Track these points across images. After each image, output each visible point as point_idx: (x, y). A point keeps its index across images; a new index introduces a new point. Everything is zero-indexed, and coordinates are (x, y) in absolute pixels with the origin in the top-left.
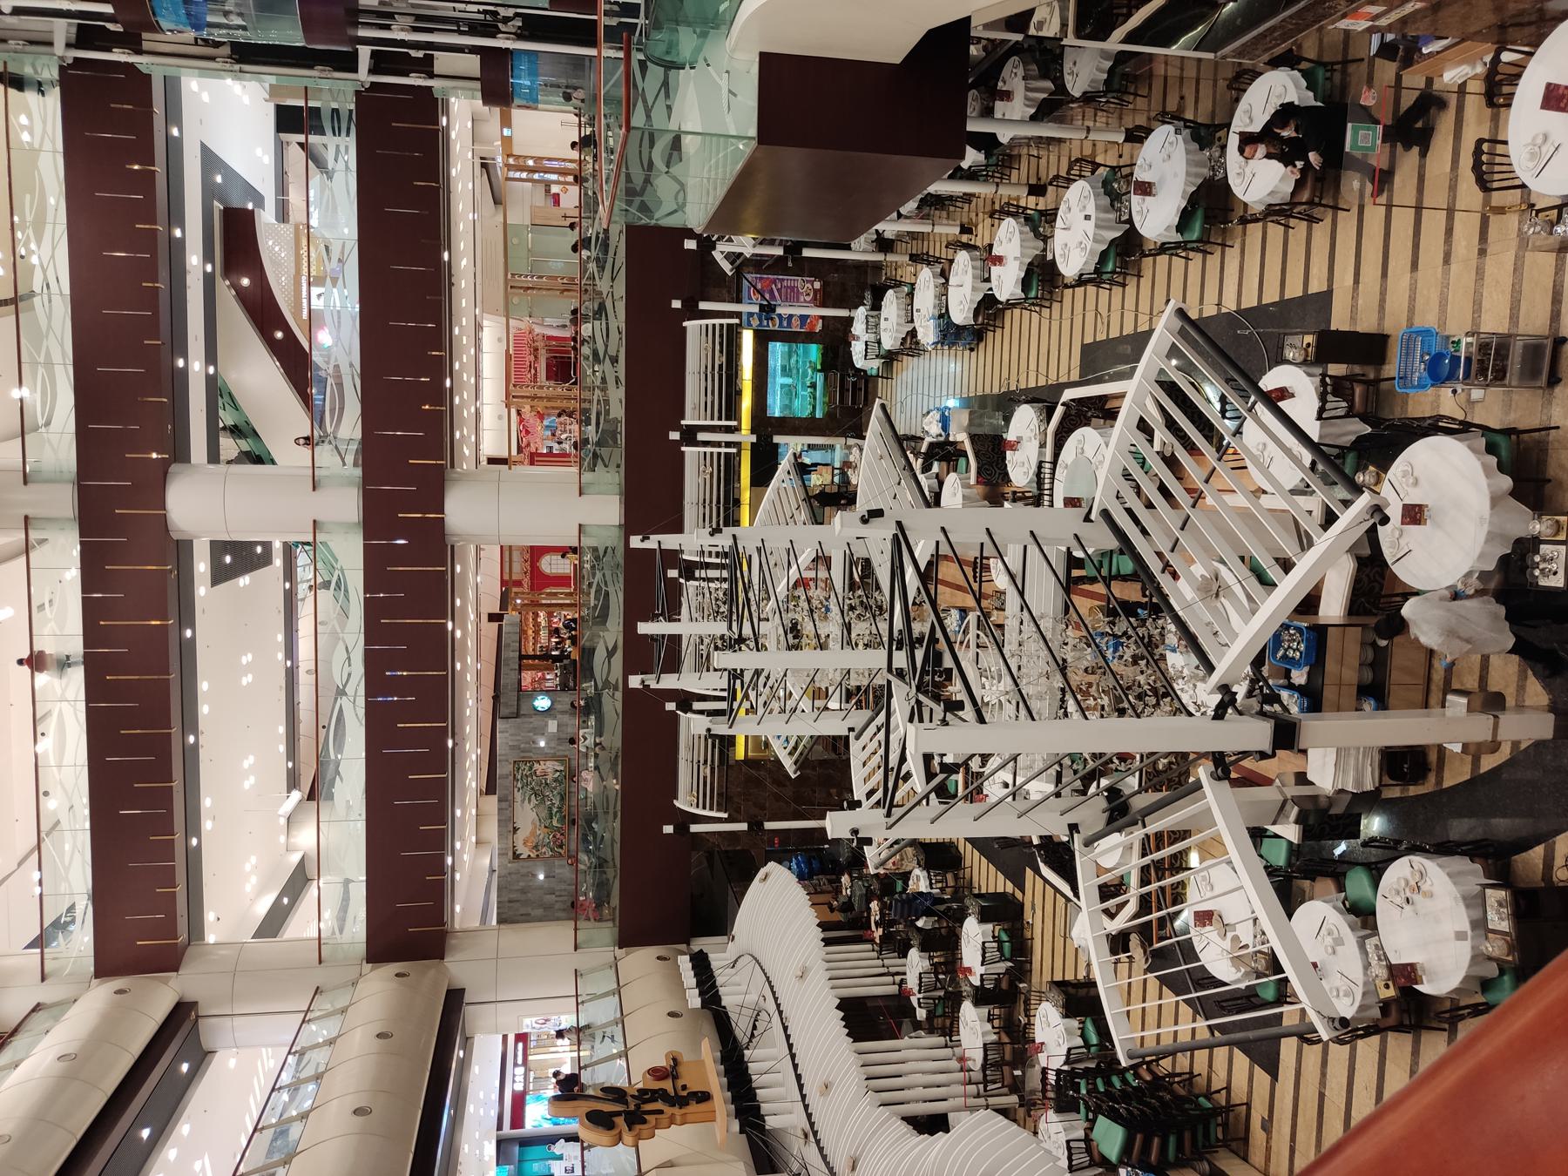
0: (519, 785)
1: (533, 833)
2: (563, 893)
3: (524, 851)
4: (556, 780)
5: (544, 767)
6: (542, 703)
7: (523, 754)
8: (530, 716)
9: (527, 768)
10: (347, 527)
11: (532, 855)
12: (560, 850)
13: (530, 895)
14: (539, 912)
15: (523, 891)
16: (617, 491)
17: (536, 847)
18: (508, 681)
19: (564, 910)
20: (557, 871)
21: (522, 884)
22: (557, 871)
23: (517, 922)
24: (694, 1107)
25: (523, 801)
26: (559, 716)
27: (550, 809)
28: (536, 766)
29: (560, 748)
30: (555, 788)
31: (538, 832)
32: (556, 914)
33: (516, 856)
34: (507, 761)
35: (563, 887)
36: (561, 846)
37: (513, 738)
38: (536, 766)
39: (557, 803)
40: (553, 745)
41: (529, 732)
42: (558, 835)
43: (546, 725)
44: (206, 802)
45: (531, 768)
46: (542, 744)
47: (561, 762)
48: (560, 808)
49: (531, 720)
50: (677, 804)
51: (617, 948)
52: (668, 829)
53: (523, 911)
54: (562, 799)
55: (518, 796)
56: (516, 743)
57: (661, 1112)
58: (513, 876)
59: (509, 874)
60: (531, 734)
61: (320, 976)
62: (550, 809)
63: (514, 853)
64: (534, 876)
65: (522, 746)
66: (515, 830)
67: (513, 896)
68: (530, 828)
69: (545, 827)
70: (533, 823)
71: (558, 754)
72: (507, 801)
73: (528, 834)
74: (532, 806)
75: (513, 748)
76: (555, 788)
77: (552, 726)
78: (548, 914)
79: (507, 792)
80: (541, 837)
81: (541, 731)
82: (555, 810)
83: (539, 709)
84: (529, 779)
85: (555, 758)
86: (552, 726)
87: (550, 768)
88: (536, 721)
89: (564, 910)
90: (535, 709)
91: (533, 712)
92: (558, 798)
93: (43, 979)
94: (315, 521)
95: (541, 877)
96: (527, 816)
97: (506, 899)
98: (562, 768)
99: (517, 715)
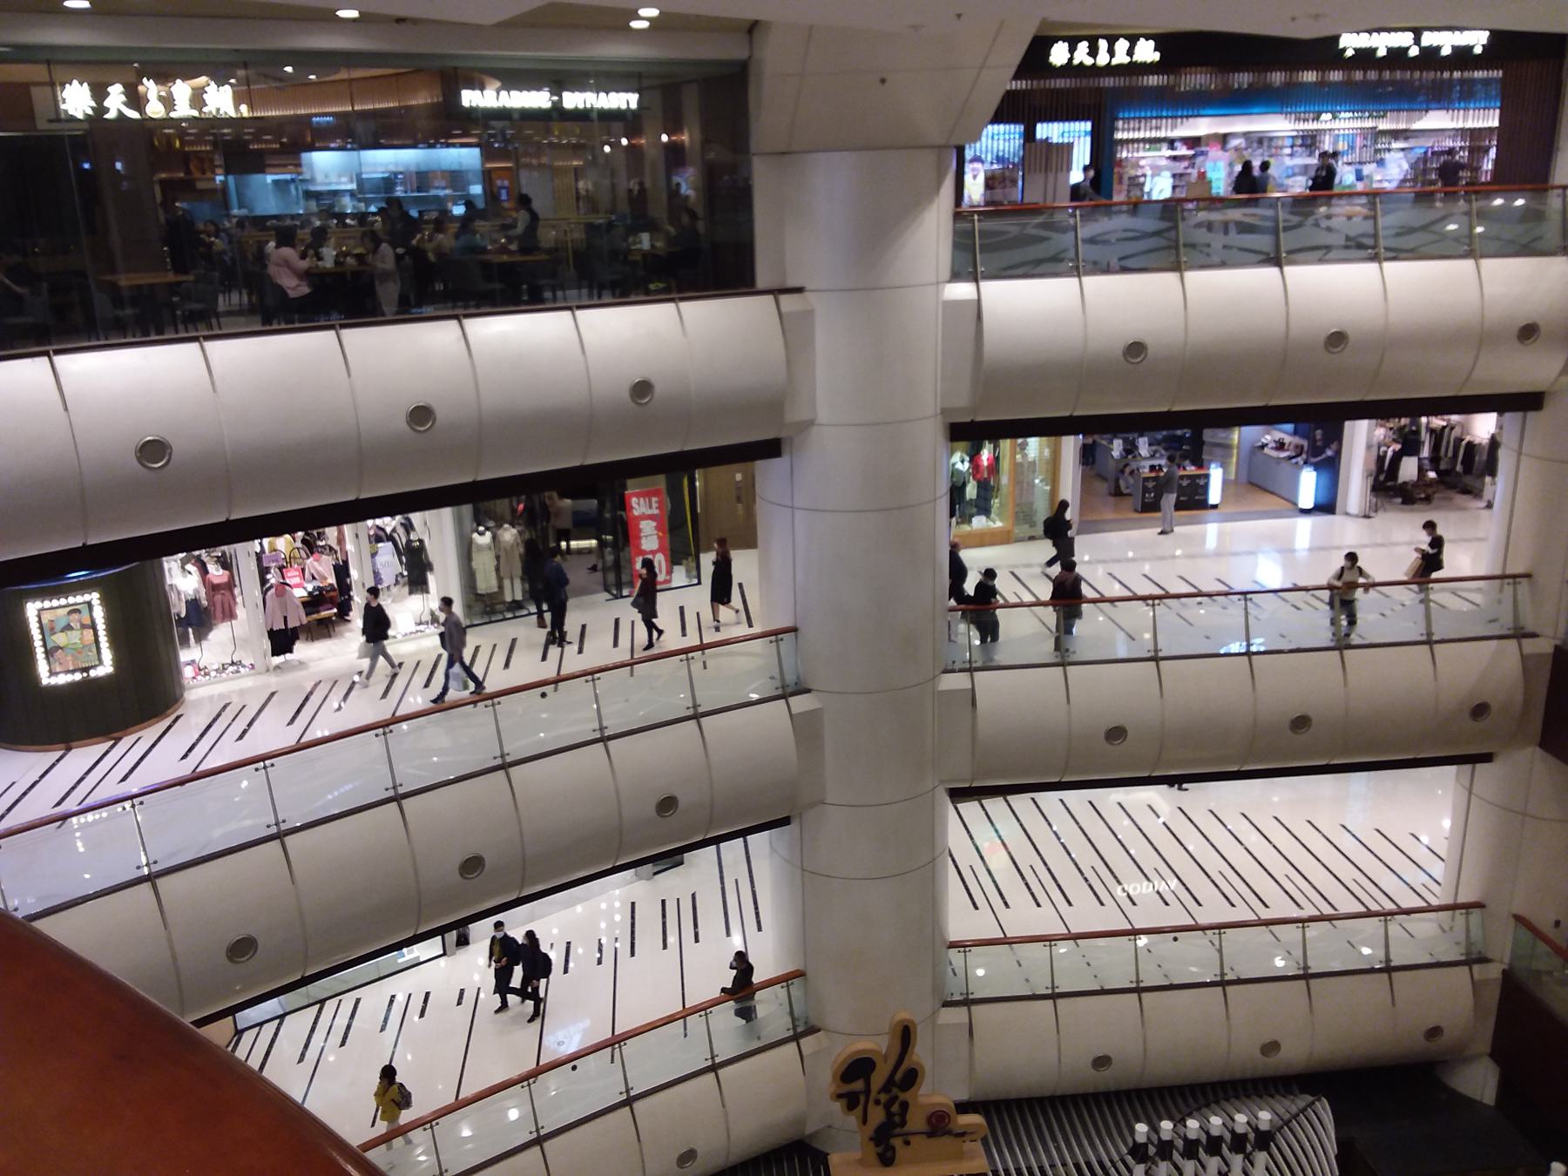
24: (872, 1150)
57: (865, 1121)
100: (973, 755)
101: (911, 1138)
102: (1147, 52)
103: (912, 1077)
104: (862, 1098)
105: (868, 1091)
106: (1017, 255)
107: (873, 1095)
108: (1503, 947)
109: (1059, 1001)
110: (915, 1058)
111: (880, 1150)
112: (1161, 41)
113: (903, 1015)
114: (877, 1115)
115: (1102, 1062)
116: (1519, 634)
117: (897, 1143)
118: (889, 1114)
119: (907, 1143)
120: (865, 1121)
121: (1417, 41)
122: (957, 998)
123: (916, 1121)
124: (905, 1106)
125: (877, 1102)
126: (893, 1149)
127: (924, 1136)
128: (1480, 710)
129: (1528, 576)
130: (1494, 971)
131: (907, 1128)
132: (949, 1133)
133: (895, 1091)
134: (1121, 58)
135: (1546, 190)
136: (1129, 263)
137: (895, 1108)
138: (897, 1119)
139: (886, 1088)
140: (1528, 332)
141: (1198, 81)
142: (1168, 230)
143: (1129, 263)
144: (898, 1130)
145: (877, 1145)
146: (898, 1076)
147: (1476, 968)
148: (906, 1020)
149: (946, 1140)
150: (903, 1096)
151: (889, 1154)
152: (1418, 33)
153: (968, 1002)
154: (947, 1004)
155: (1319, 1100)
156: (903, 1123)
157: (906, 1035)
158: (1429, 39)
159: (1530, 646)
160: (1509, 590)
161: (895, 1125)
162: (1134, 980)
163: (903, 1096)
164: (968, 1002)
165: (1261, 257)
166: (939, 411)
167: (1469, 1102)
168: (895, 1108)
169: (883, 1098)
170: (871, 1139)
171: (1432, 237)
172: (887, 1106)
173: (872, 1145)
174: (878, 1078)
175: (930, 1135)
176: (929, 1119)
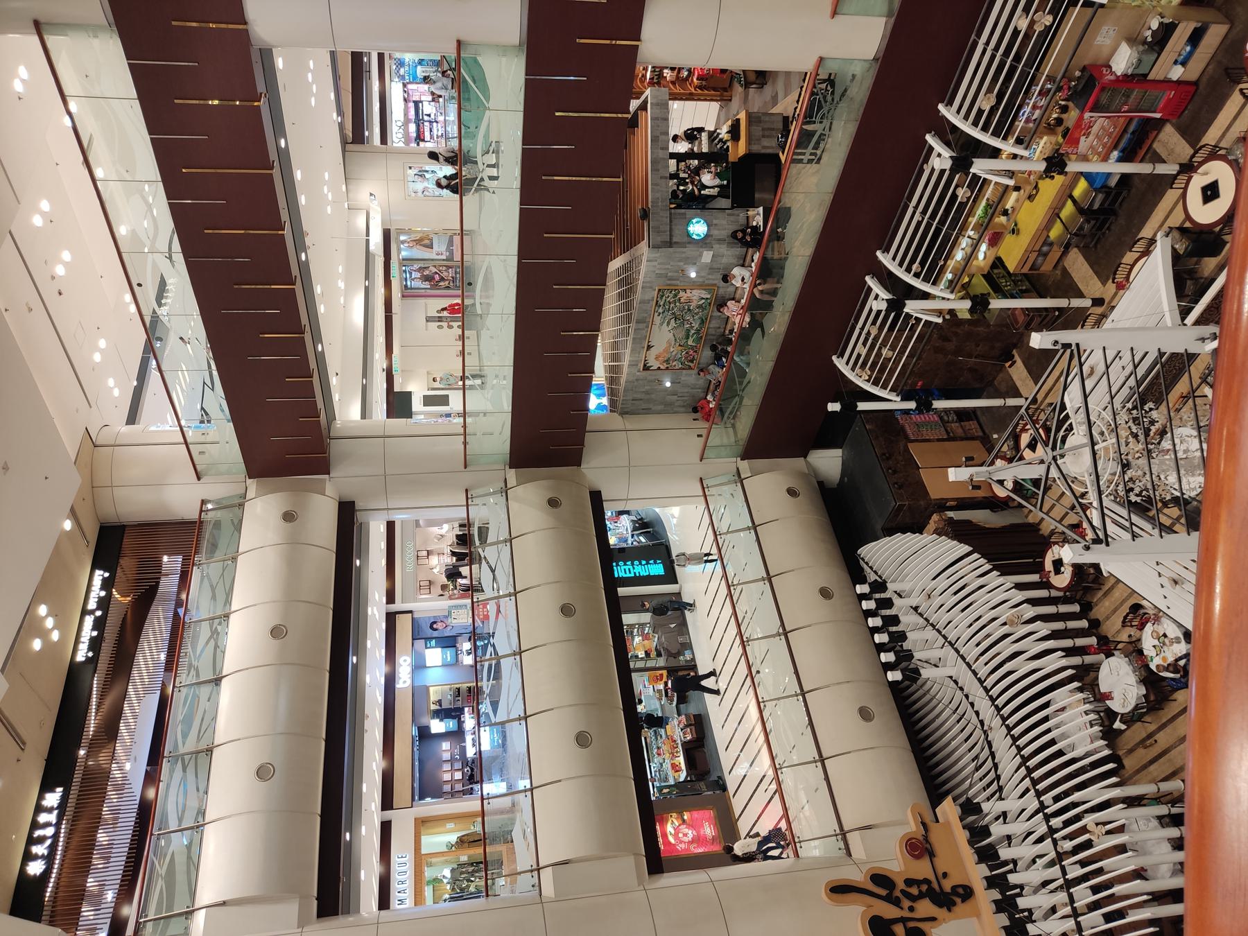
0: (661, 310)
1: (666, 350)
2: (686, 394)
3: (654, 364)
4: (699, 307)
5: (689, 295)
6: (698, 228)
7: (669, 282)
8: (682, 245)
9: (671, 295)
10: (503, 49)
11: (662, 367)
12: (690, 364)
13: (653, 396)
14: (660, 407)
15: (647, 393)
16: (885, 9)
17: (667, 361)
18: (658, 195)
19: (684, 406)
20: (683, 379)
21: (647, 388)
22: (683, 379)
23: (639, 414)
24: (960, 907)
25: (662, 324)
26: (716, 246)
27: (688, 331)
28: (682, 294)
29: (710, 277)
30: (696, 314)
31: (672, 350)
32: (675, 409)
33: (646, 368)
34: (651, 288)
35: (686, 390)
36: (692, 361)
37: (661, 266)
38: (682, 294)
39: (696, 325)
40: (703, 274)
41: (680, 261)
42: (691, 352)
43: (701, 255)
44: (318, 290)
45: (675, 296)
46: (693, 275)
47: (709, 291)
48: (698, 331)
49: (684, 250)
50: (840, 363)
51: (739, 459)
52: (834, 407)
53: (644, 406)
54: (703, 322)
55: (658, 320)
56: (663, 272)
57: (933, 919)
58: (640, 382)
59: (637, 380)
60: (682, 264)
61: (467, 478)
62: (688, 331)
63: (645, 365)
64: (660, 382)
65: (669, 274)
66: (649, 347)
67: (639, 396)
68: (664, 345)
69: (680, 345)
70: (669, 342)
71: (707, 282)
72: (645, 322)
73: (661, 350)
74: (670, 327)
75: (659, 276)
76: (696, 314)
77: (707, 256)
78: (668, 408)
79: (646, 315)
80: (674, 353)
81: (693, 261)
82: (693, 332)
83: (694, 237)
84: (672, 305)
85: (702, 286)
86: (707, 256)
87: (696, 296)
88: (690, 251)
89: (684, 406)
90: (689, 235)
91: (686, 239)
92: (699, 321)
93: (199, 479)
94: (459, 42)
95: (668, 384)
96: (663, 337)
97: (631, 398)
98: (709, 297)
99: (670, 244)
100: (603, 858)
101: (940, 875)
102: (52, 799)
103: (881, 879)
104: (911, 924)
105: (903, 920)
106: (181, 878)
107: (906, 914)
108: (731, 463)
109: (825, 755)
110: (862, 880)
111: (958, 900)
112: (46, 787)
113: (823, 894)
114: (925, 907)
115: (865, 714)
116: (505, 491)
117: (947, 885)
118: (921, 896)
119: (945, 875)
120: (933, 919)
121: (92, 612)
122: (842, 845)
123: (922, 869)
124: (909, 882)
125: (911, 909)
126: (954, 888)
127: (935, 860)
128: (553, 503)
129: (467, 490)
130: (744, 465)
131: (932, 877)
132: (926, 838)
133: (897, 893)
134: (52, 818)
135: (201, 522)
136: (202, 789)
137: (914, 891)
138: (924, 888)
139: (896, 903)
140: (288, 517)
141: (122, 758)
142: (183, 760)
143: (202, 789)
144: (935, 885)
145: (954, 904)
146: (883, 892)
147: (743, 476)
148: (826, 892)
149: (934, 838)
150: (901, 885)
151: (961, 891)
152: (85, 612)
153: (843, 834)
154: (849, 854)
155: (860, 555)
156: (927, 881)
157: (840, 890)
158: (92, 605)
159: (512, 481)
160: (476, 501)
161: (930, 889)
162: (765, 699)
163: (901, 885)
164: (843, 834)
165: (214, 693)
166: (300, 930)
167: (844, 464)
168: (914, 891)
169: (906, 903)
170: (949, 910)
171: (220, 586)
172: (914, 899)
173: (955, 909)
174: (888, 911)
175: (932, 855)
176: (917, 857)
